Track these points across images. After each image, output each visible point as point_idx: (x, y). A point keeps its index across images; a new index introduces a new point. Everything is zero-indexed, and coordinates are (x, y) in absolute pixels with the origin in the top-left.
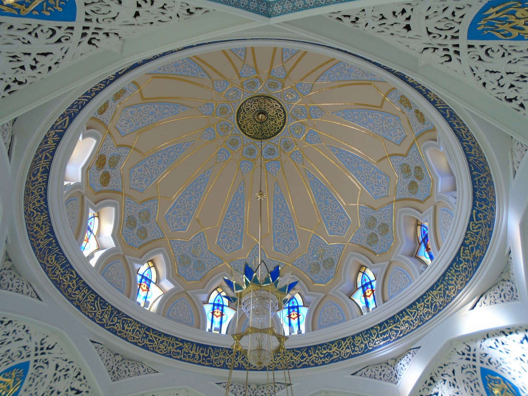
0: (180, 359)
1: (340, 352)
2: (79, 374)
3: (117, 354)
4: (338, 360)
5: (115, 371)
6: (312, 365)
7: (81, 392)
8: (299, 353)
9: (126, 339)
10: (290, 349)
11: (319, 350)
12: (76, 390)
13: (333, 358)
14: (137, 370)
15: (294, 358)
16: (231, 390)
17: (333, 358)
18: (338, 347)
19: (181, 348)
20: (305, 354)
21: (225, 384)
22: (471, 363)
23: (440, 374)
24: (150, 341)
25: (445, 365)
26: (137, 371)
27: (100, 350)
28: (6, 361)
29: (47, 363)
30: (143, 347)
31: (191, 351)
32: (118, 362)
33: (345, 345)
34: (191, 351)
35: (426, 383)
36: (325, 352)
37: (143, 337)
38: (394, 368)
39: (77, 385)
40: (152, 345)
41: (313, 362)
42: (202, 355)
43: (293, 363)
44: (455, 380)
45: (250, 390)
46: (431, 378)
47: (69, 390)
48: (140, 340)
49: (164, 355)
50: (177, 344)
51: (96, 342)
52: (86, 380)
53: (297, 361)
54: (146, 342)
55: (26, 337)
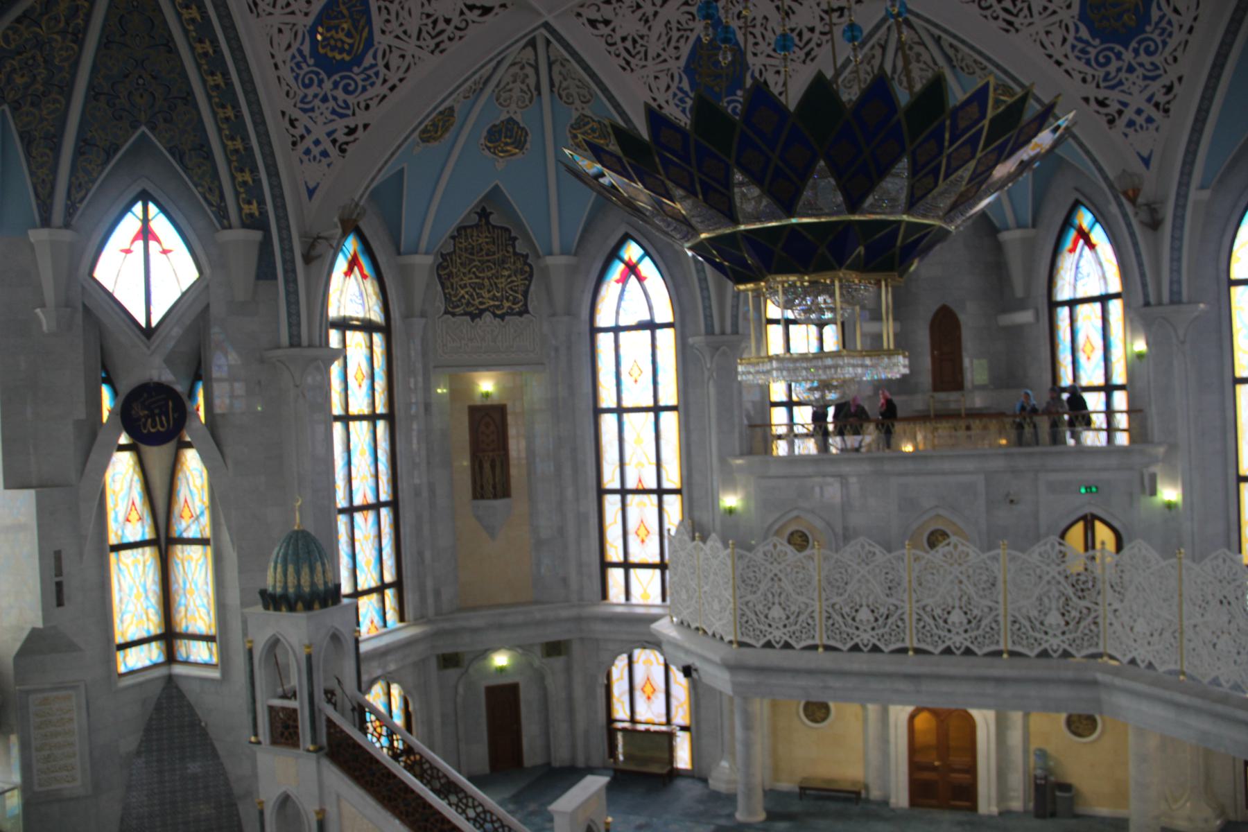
12: (478, 8)
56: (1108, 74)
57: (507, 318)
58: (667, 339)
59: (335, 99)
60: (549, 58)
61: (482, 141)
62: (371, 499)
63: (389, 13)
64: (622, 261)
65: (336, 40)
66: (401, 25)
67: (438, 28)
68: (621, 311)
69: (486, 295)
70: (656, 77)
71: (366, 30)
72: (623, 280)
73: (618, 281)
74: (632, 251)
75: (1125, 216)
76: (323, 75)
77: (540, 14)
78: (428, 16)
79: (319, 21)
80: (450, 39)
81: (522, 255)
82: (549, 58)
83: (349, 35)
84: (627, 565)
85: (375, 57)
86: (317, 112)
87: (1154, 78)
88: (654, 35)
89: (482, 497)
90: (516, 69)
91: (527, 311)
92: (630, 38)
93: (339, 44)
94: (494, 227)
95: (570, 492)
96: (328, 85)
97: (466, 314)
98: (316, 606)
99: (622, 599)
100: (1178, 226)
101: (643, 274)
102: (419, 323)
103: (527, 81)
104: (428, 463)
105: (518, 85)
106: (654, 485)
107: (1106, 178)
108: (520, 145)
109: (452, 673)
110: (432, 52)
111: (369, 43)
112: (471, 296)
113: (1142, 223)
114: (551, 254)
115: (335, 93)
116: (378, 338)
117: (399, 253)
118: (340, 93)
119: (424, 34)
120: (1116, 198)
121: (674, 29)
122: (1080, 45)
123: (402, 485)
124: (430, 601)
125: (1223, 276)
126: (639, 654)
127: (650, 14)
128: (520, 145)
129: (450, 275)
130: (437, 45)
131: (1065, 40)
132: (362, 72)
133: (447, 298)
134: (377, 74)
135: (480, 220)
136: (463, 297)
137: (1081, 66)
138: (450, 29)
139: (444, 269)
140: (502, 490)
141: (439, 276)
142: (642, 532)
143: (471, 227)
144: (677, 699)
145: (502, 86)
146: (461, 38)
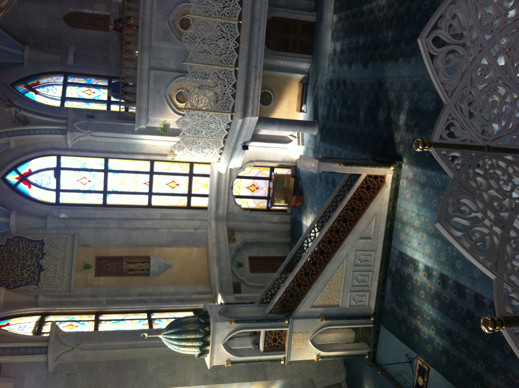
57: (44, 252)
58: (66, 161)
62: (147, 321)
64: (18, 183)
68: (48, 187)
69: (29, 263)
72: (29, 184)
73: (30, 187)
74: (12, 177)
81: (7, 241)
84: (189, 195)
89: (149, 270)
91: (42, 240)
95: (149, 223)
98: (208, 320)
99: (207, 199)
101: (27, 171)
104: (127, 296)
106: (148, 176)
109: (243, 287)
112: (28, 270)
114: (8, 223)
123: (138, 307)
124: (204, 296)
126: (235, 193)
129: (14, 282)
133: (28, 284)
136: (28, 275)
140: (147, 259)
141: (14, 288)
142: (173, 185)
144: (258, 173)
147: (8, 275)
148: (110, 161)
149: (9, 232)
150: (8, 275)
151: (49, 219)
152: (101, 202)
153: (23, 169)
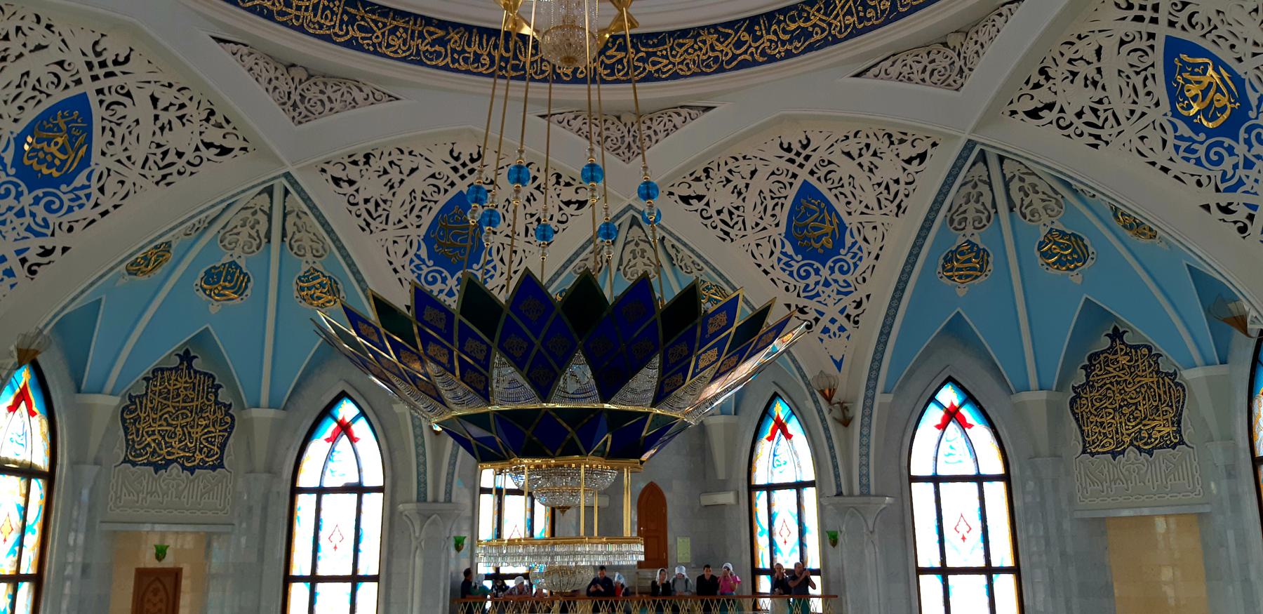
0: (446, 68)
1: (830, 25)
2: (212, 113)
3: (293, 65)
4: (825, 43)
5: (298, 103)
6: (761, 59)
7: (231, 150)
8: (730, 35)
9: (301, 29)
10: (708, 27)
11: (779, 23)
12: (217, 147)
13: (812, 40)
14: (348, 97)
15: (719, 47)
16: (576, 128)
17: (812, 40)
18: (824, 14)
19: (442, 42)
20: (746, 37)
21: (560, 118)
22: (1146, 27)
23: (1066, 58)
24: (361, 28)
25: (1079, 37)
26: (349, 99)
27: (245, 58)
28: (33, 98)
29: (128, 94)
30: (348, 44)
31: (469, 46)
32: (300, 82)
33: (842, 7)
34: (469, 46)
35: (1027, 83)
36: (793, 26)
37: (342, 20)
38: (959, 55)
39: (214, 136)
40: (370, 38)
41: (763, 53)
42: (496, 54)
43: (716, 59)
44: (1099, 71)
45: (621, 126)
46: (1043, 71)
47: (201, 147)
48: (337, 30)
49: (404, 59)
50: (431, 34)
51: (230, 42)
52: (231, 126)
53: (727, 54)
54: (354, 32)
55: (53, 41)
56: (807, 286)
58: (374, 503)
59: (33, 215)
60: (285, 207)
61: (198, 281)
63: (113, 136)
64: (335, 419)
65: (46, 154)
66: (126, 149)
67: (168, 160)
68: (327, 472)
70: (395, 242)
71: (84, 148)
72: (333, 439)
73: (328, 440)
75: (820, 411)
76: (23, 187)
77: (283, 164)
78: (159, 146)
79: (29, 130)
80: (180, 173)
81: (225, 405)
82: (285, 207)
83: (63, 150)
85: (89, 178)
86: (9, 226)
87: (847, 294)
88: (398, 201)
90: (248, 213)
91: (221, 466)
92: (373, 201)
93: (49, 158)
94: (196, 372)
96: (27, 199)
97: (149, 464)
100: (866, 424)
101: (356, 435)
102: (89, 471)
103: (257, 227)
105: (247, 229)
107: (804, 376)
108: (240, 291)
110: (157, 183)
111: (85, 162)
112: (159, 444)
113: (835, 419)
114: (258, 406)
115: (35, 209)
116: (37, 486)
117: (79, 391)
118: (40, 211)
119: (150, 163)
120: (812, 394)
121: (419, 199)
122: (785, 259)
125: (905, 472)
127: (396, 180)
128: (240, 291)
129: (137, 420)
130: (164, 177)
131: (772, 253)
132: (71, 192)
134: (88, 196)
135: (181, 363)
136: (149, 445)
137: (785, 277)
138: (180, 164)
139: (130, 413)
141: (124, 420)
143: (171, 369)
145: (228, 228)
146: (192, 174)
147: (152, 409)
148: (373, 586)
149: (243, 408)
150: (152, 409)
151: (265, 476)
152: (295, 571)
153: (361, 428)
